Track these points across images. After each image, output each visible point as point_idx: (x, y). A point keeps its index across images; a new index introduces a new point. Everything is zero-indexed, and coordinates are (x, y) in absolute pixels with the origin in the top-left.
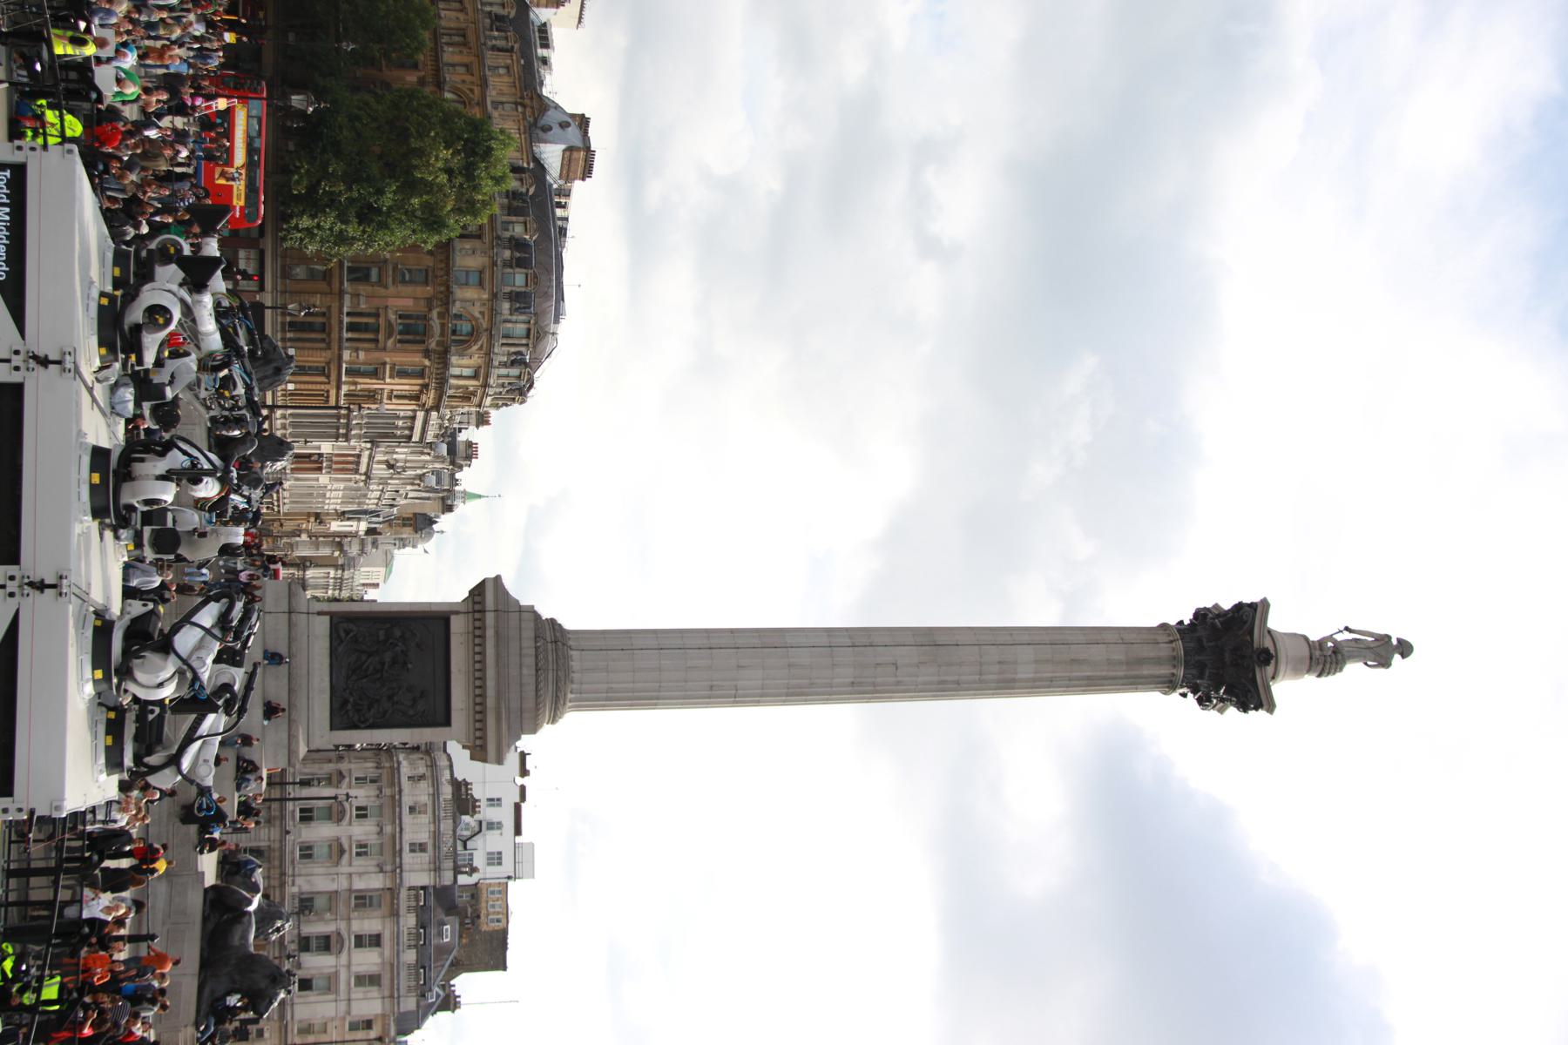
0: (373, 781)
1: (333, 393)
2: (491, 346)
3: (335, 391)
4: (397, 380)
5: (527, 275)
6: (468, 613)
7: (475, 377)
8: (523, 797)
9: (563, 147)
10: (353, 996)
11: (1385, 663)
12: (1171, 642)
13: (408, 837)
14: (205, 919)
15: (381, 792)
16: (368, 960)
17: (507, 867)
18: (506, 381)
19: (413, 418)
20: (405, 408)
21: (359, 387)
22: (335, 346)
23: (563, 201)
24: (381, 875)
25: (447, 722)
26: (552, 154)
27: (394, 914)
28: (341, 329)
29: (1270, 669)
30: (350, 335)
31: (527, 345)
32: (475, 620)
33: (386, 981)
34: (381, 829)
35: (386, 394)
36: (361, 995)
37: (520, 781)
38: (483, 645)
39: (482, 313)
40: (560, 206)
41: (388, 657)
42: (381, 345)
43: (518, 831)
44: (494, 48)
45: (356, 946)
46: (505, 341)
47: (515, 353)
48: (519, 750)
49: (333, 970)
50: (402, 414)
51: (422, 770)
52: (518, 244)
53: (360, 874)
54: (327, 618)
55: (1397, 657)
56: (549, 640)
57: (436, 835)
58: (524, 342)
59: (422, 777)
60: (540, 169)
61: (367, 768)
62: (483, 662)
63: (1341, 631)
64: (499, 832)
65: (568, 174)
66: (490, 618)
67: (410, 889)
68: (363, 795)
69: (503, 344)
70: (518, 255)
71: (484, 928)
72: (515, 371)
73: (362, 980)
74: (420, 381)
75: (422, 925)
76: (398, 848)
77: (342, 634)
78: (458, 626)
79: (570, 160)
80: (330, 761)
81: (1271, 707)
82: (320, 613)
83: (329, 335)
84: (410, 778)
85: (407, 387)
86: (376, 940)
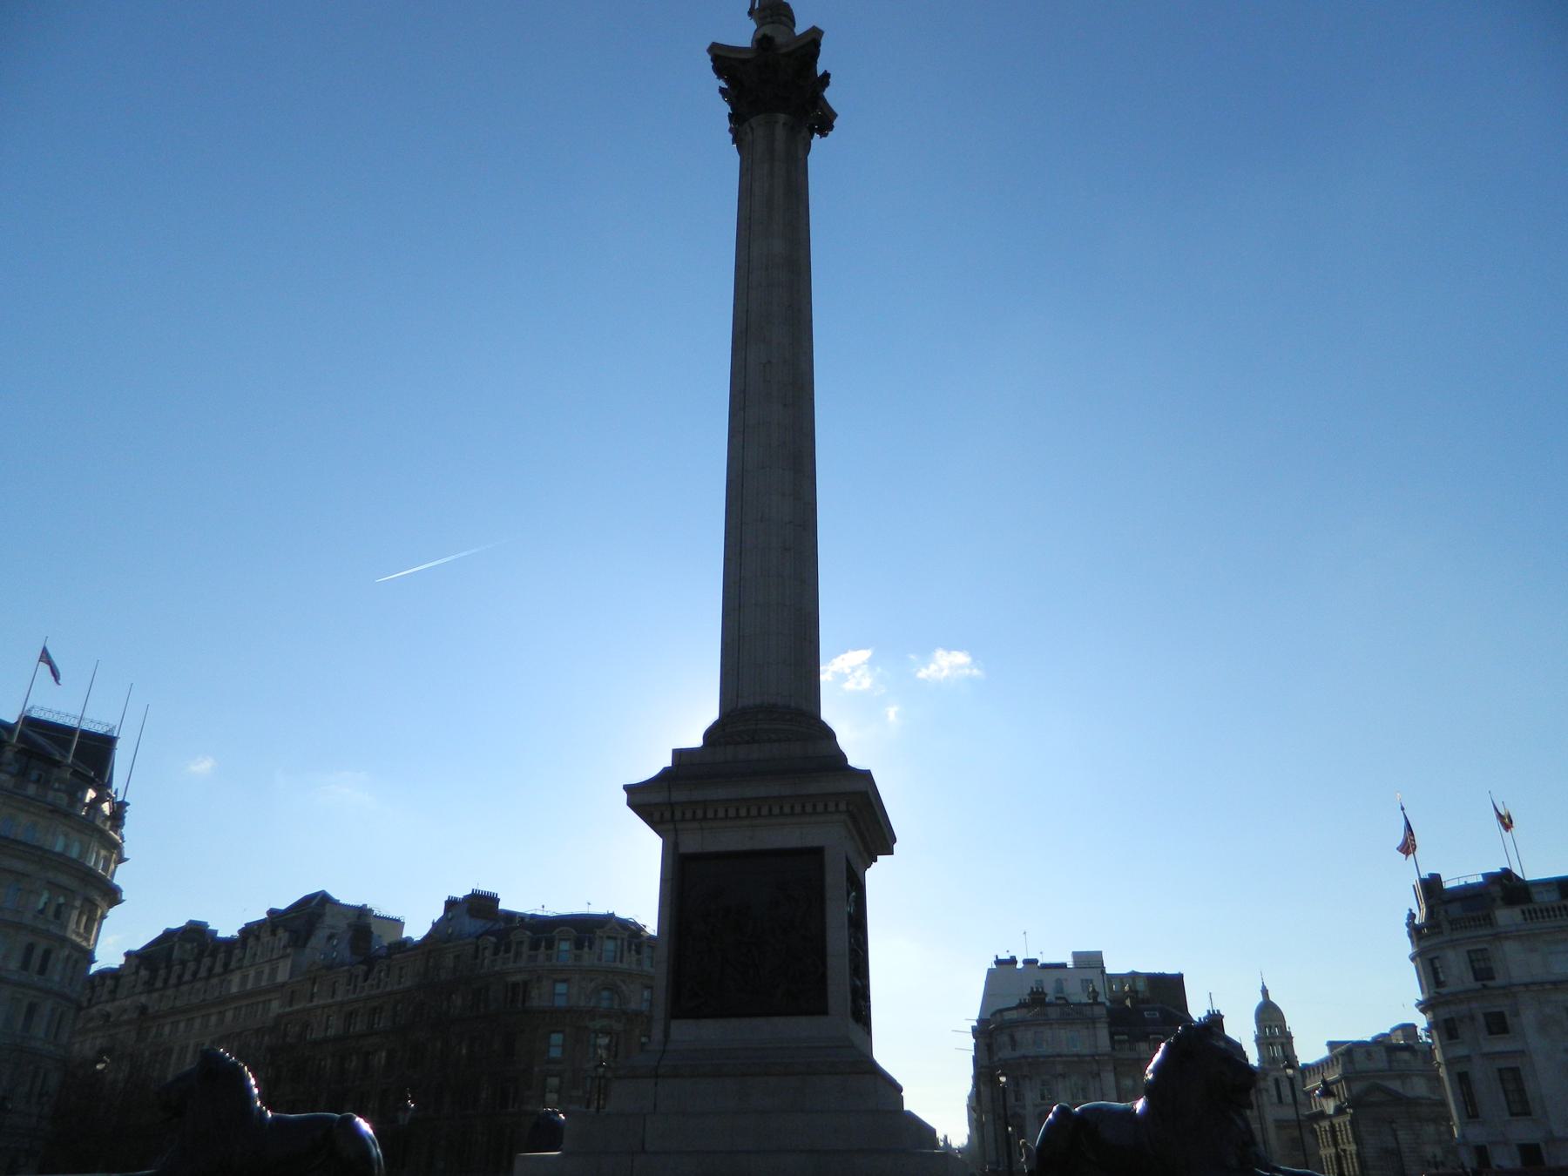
5: (561, 940)
6: (676, 830)
15: (1026, 1076)
17: (1092, 974)
24: (1102, 1075)
26: (471, 925)
31: (623, 939)
34: (1061, 1075)
37: (1020, 965)
39: (592, 980)
43: (1063, 966)
46: (618, 959)
47: (630, 950)
48: (994, 967)
51: (1005, 1039)
54: (675, 1024)
58: (619, 942)
59: (1012, 1038)
64: (1065, 983)
67: (1113, 1048)
70: (543, 949)
76: (1076, 1059)
78: (692, 843)
84: (1014, 1049)
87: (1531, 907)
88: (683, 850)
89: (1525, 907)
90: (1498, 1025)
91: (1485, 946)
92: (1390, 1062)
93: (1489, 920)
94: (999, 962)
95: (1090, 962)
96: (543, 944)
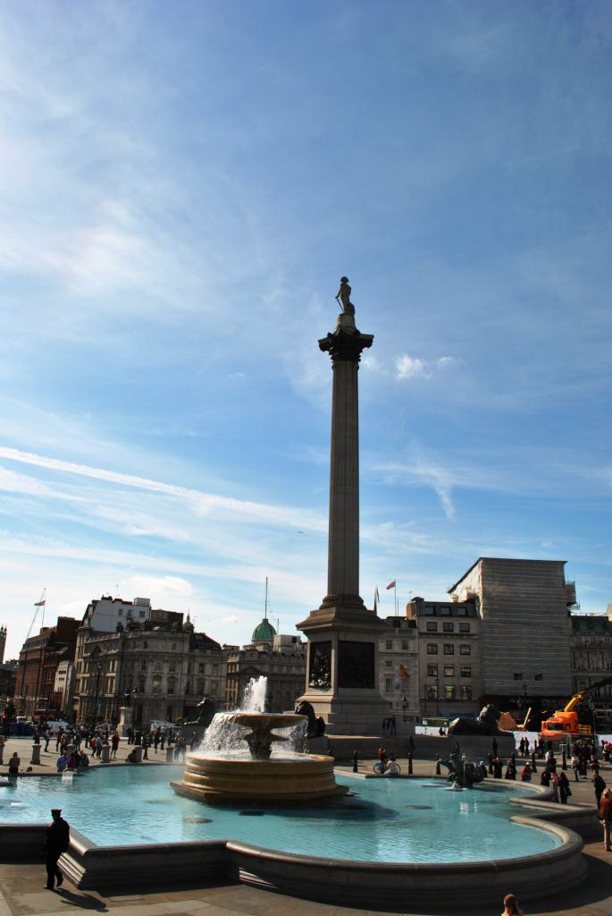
0: (145, 662)
8: (120, 600)
11: (350, 289)
13: (170, 651)
17: (146, 609)
43: (130, 603)
51: (142, 643)
53: (182, 670)
57: (171, 639)
59: (145, 643)
61: (137, 666)
68: (151, 669)
71: (167, 621)
75: (197, 647)
78: (342, 639)
80: (131, 681)
81: (372, 336)
84: (145, 647)
86: (202, 665)
94: (103, 598)
95: (144, 603)
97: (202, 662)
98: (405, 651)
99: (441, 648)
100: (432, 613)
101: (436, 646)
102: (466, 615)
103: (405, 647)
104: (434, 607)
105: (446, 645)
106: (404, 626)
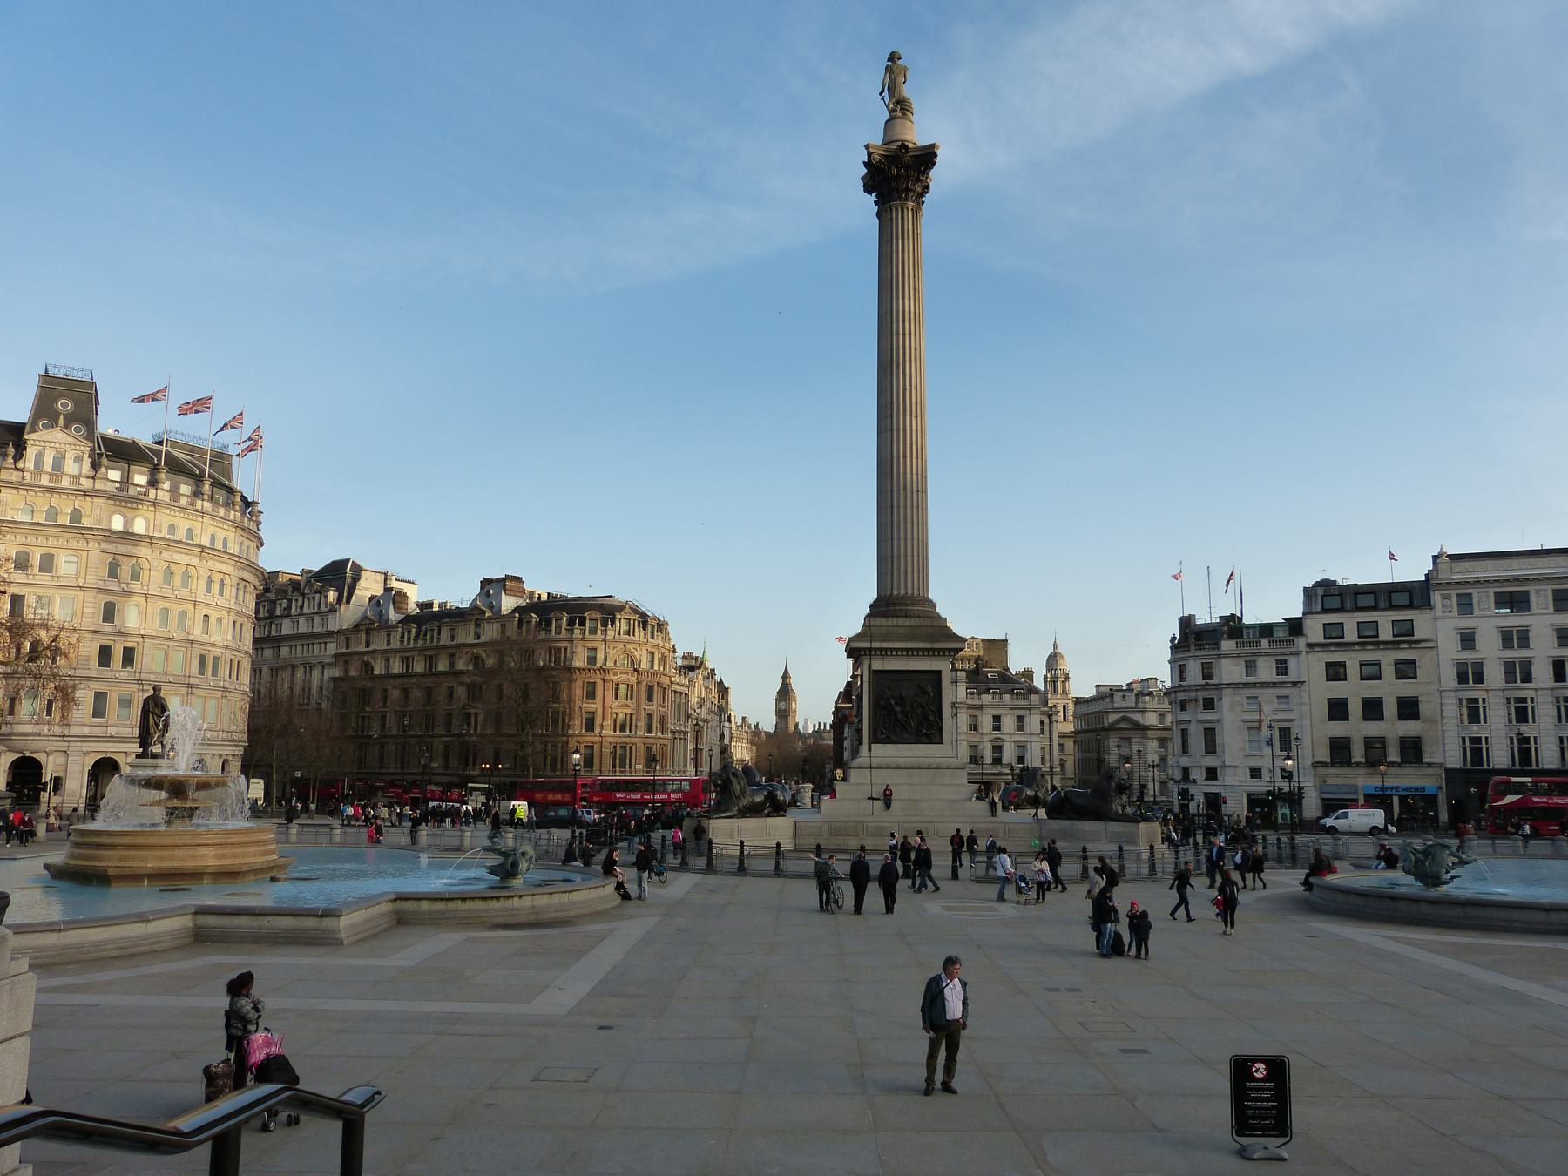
1: (662, 741)
2: (634, 642)
3: (660, 740)
4: (655, 702)
7: (653, 654)
9: (503, 593)
10: (1028, 732)
12: (891, 210)
14: (1069, 818)
16: (1008, 723)
18: (656, 633)
19: (675, 692)
20: (670, 696)
21: (658, 725)
22: (634, 740)
23: (537, 596)
24: (959, 715)
25: (938, 673)
26: (508, 603)
27: (981, 707)
28: (625, 737)
29: (911, 145)
30: (628, 731)
31: (634, 620)
32: (876, 655)
33: (1020, 713)
35: (663, 709)
36: (1028, 728)
38: (891, 650)
39: (614, 648)
40: (539, 598)
41: (898, 709)
42: (634, 712)
44: (439, 639)
45: (1000, 730)
49: (1013, 744)
50: (673, 699)
52: (571, 623)
54: (873, 745)
55: (900, 62)
56: (885, 609)
58: (632, 622)
60: (517, 609)
62: (902, 650)
63: (883, 98)
65: (520, 592)
66: (876, 645)
69: (634, 635)
70: (577, 625)
72: (649, 627)
73: (1020, 728)
74: (656, 687)
75: (987, 691)
77: (884, 736)
78: (878, 665)
79: (512, 591)
82: (870, 750)
83: (627, 743)
85: (659, 696)
86: (997, 718)
87: (1241, 640)
88: (873, 668)
89: (1239, 640)
90: (1209, 704)
91: (1210, 661)
92: (1137, 702)
93: (1217, 645)
96: (577, 622)
97: (996, 712)
98: (1282, 678)
99: (1353, 670)
100: (1339, 606)
101: (1343, 665)
102: (1410, 606)
103: (1282, 669)
104: (1341, 595)
105: (1362, 664)
106: (1280, 634)
